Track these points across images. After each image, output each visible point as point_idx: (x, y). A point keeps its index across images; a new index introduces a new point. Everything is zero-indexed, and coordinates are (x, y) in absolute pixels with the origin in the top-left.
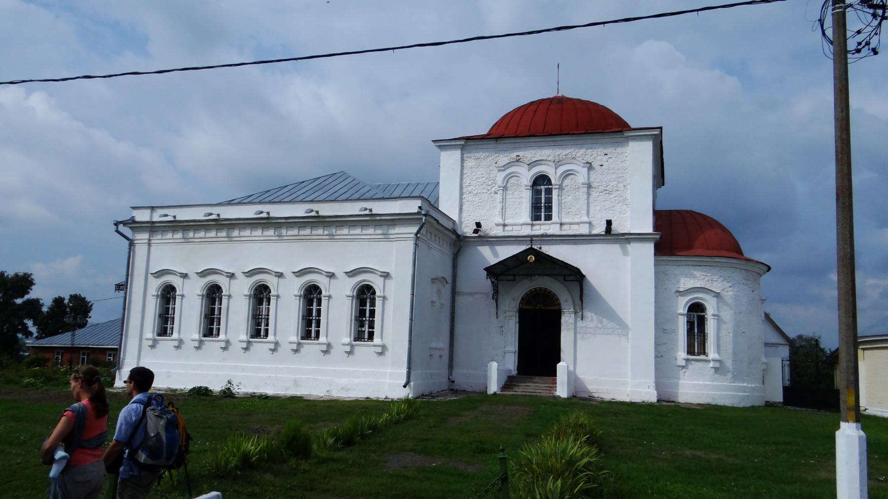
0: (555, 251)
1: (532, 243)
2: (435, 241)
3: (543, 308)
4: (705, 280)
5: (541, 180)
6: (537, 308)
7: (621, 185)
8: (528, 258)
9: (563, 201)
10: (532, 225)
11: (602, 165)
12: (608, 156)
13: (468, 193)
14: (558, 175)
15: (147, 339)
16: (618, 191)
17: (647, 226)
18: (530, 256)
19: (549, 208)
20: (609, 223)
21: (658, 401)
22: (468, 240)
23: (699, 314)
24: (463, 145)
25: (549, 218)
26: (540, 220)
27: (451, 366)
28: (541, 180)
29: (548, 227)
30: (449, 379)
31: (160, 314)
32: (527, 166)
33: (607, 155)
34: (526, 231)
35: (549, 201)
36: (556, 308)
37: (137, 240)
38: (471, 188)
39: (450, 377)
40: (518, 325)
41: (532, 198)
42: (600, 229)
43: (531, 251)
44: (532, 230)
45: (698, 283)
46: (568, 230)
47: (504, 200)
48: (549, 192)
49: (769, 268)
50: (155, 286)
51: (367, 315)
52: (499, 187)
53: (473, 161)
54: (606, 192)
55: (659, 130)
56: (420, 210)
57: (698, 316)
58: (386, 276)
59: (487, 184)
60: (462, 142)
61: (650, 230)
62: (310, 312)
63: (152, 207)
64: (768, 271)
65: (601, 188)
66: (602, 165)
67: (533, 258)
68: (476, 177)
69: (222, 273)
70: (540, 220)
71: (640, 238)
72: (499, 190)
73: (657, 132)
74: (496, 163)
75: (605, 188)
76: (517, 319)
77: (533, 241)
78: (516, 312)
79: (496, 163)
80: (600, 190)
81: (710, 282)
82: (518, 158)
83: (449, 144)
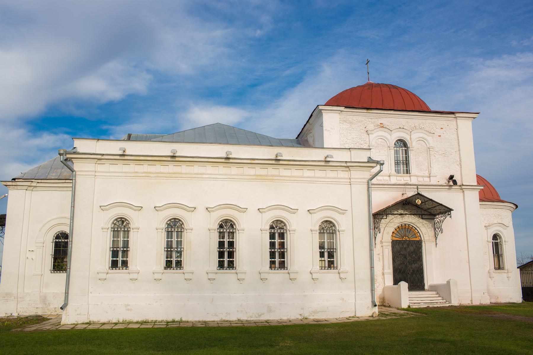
1: (418, 190)
6: (404, 239)
16: (452, 155)
18: (419, 200)
20: (451, 177)
21: (491, 303)
24: (341, 111)
25: (408, 172)
28: (402, 143)
34: (394, 180)
36: (417, 239)
42: (444, 181)
48: (406, 152)
54: (444, 155)
58: (342, 212)
61: (476, 184)
66: (440, 136)
67: (420, 202)
71: (470, 187)
74: (365, 128)
77: (418, 189)
79: (365, 128)
83: (331, 109)
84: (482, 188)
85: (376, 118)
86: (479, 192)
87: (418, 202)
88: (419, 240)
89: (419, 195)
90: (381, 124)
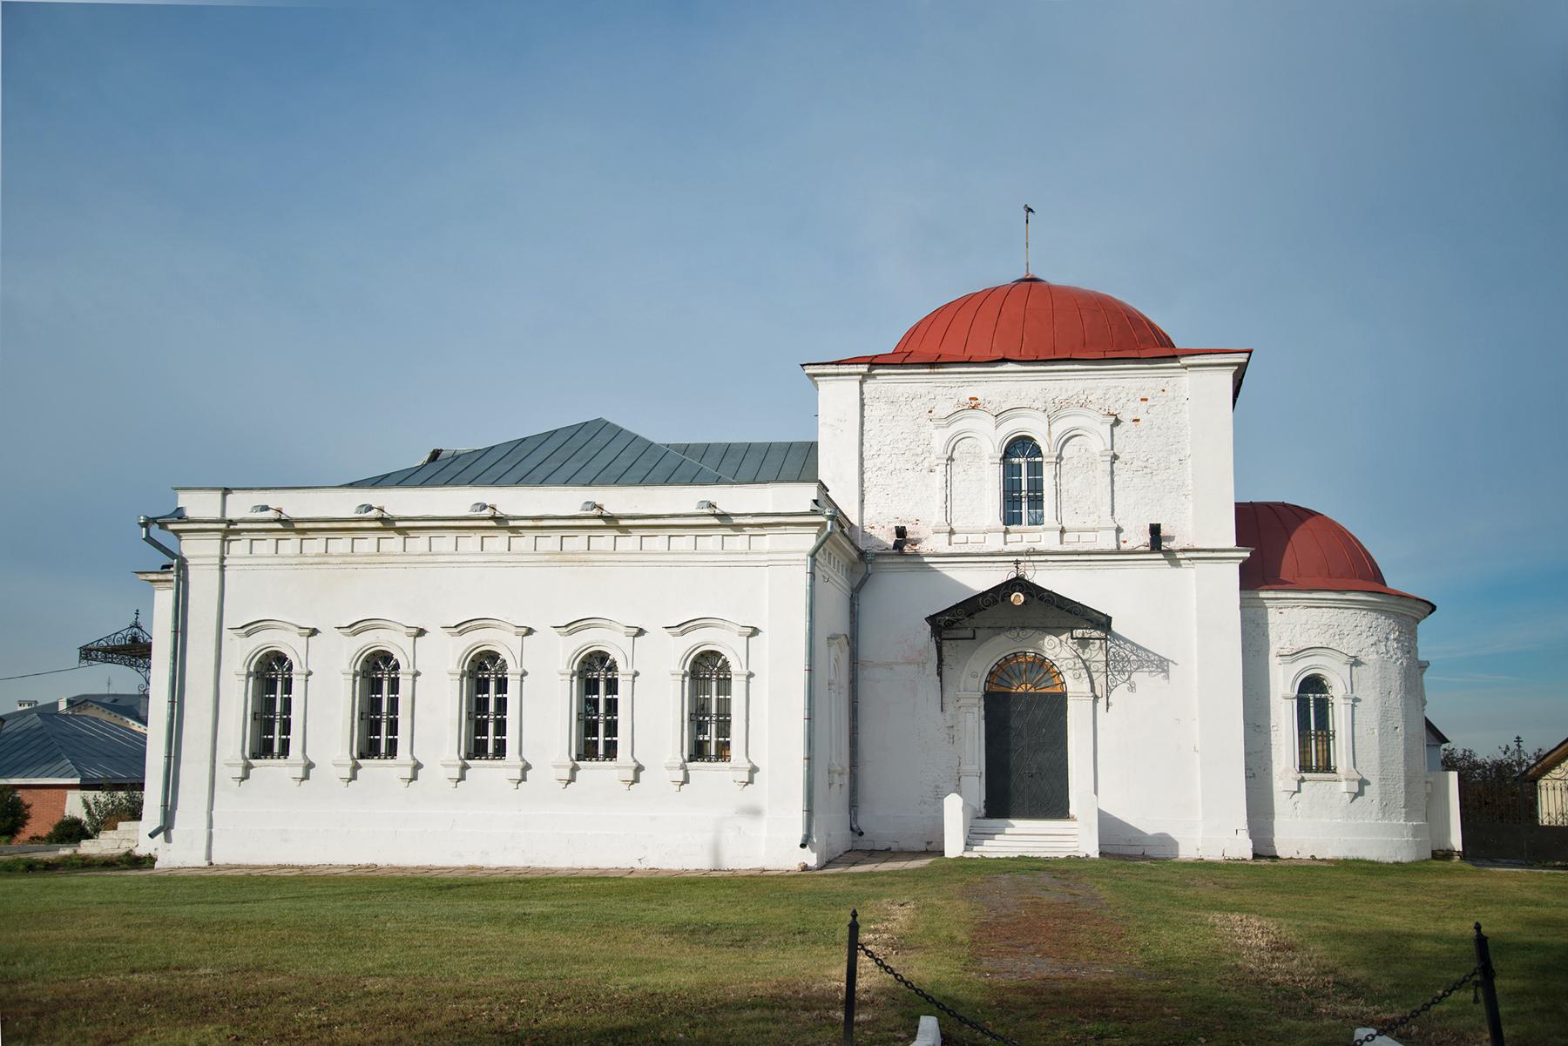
0: (1046, 578)
2: (829, 563)
3: (1033, 690)
4: (1328, 635)
5: (1020, 446)
7: (1174, 458)
8: (1012, 600)
9: (1064, 487)
10: (1006, 532)
11: (1137, 420)
12: (1149, 403)
13: (874, 469)
14: (1054, 437)
15: (229, 765)
17: (1226, 535)
19: (1037, 501)
22: (880, 560)
23: (1318, 696)
24: (863, 375)
25: (1037, 521)
26: (1021, 523)
27: (853, 804)
28: (1020, 446)
29: (1035, 536)
30: (852, 829)
31: (255, 713)
32: (993, 418)
33: (1146, 400)
34: (995, 543)
35: (1036, 486)
37: (194, 557)
38: (882, 459)
39: (854, 826)
40: (983, 722)
41: (1004, 482)
43: (1019, 583)
44: (1006, 543)
45: (1317, 639)
46: (1072, 542)
47: (948, 483)
48: (1036, 469)
49: (1433, 608)
50: (240, 655)
51: (602, 709)
52: (937, 458)
53: (883, 406)
55: (1247, 355)
56: (816, 508)
57: (1315, 699)
59: (913, 452)
60: (864, 369)
62: (482, 705)
63: (226, 489)
64: (1431, 613)
65: (1136, 463)
66: (1137, 420)
68: (889, 438)
69: (286, 625)
70: (1021, 523)
72: (938, 465)
73: (1242, 358)
74: (930, 412)
75: (1145, 464)
76: (983, 713)
78: (980, 699)
79: (930, 412)
80: (1134, 467)
81: (1337, 637)
82: (974, 402)
83: (836, 371)
84: (1253, 549)
85: (959, 384)
86: (1241, 566)
87: (1017, 599)
88: (1060, 691)
89: (1019, 583)
90: (971, 399)
